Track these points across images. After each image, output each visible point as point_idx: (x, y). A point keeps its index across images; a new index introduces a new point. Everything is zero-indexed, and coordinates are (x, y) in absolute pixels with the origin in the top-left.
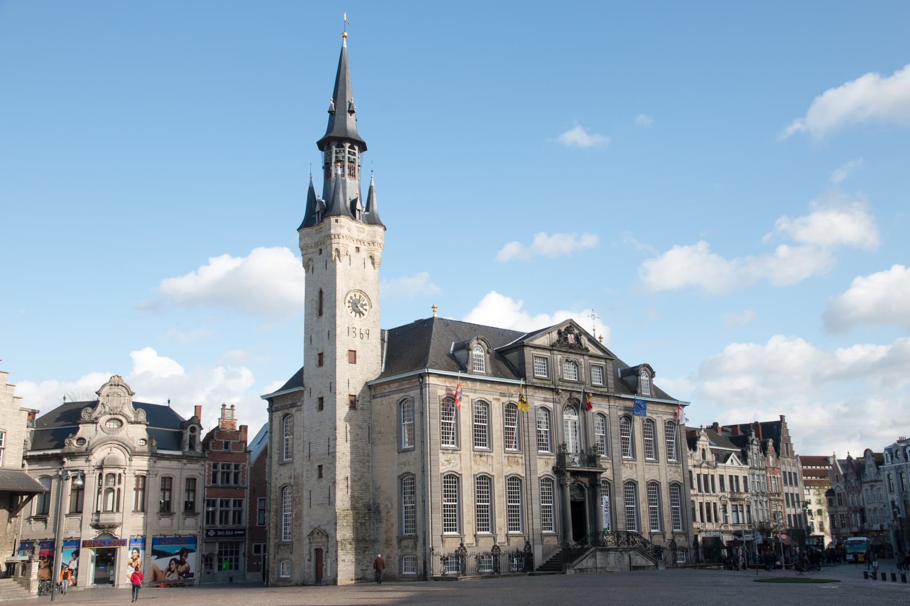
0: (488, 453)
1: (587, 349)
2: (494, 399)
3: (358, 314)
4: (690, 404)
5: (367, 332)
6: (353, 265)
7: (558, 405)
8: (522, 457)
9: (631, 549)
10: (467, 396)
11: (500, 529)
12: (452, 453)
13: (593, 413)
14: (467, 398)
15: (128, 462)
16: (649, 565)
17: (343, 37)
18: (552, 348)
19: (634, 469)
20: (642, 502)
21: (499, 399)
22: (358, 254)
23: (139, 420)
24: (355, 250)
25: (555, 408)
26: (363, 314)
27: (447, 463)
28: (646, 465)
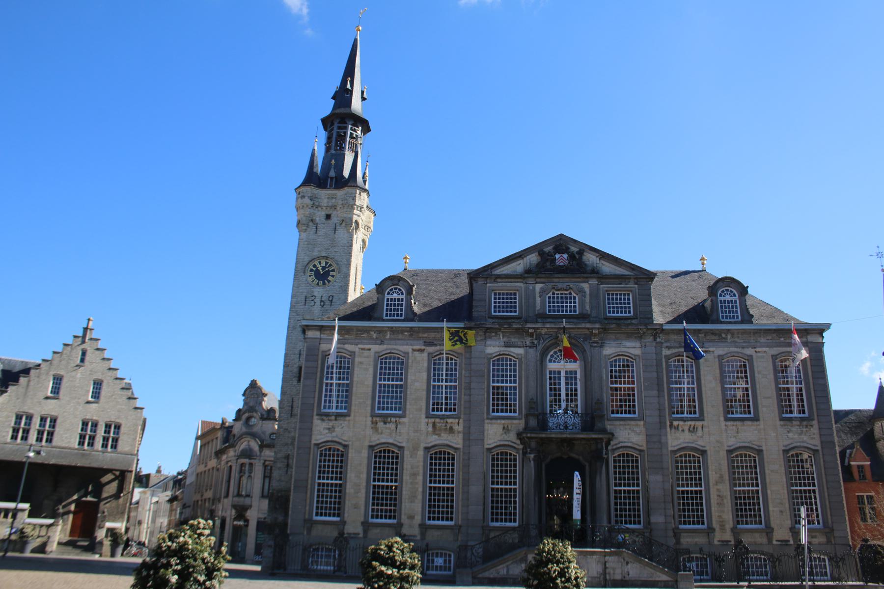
0: (397, 419)
2: (414, 350)
3: (321, 283)
4: (832, 327)
5: (331, 298)
6: (321, 232)
7: (532, 351)
8: (458, 423)
11: (411, 517)
12: (336, 420)
13: (605, 355)
14: (368, 351)
16: (660, 579)
17: (357, 31)
18: (530, 273)
19: (700, 433)
20: (717, 483)
21: (424, 350)
22: (329, 221)
24: (323, 218)
25: (526, 353)
26: (329, 281)
27: (327, 431)
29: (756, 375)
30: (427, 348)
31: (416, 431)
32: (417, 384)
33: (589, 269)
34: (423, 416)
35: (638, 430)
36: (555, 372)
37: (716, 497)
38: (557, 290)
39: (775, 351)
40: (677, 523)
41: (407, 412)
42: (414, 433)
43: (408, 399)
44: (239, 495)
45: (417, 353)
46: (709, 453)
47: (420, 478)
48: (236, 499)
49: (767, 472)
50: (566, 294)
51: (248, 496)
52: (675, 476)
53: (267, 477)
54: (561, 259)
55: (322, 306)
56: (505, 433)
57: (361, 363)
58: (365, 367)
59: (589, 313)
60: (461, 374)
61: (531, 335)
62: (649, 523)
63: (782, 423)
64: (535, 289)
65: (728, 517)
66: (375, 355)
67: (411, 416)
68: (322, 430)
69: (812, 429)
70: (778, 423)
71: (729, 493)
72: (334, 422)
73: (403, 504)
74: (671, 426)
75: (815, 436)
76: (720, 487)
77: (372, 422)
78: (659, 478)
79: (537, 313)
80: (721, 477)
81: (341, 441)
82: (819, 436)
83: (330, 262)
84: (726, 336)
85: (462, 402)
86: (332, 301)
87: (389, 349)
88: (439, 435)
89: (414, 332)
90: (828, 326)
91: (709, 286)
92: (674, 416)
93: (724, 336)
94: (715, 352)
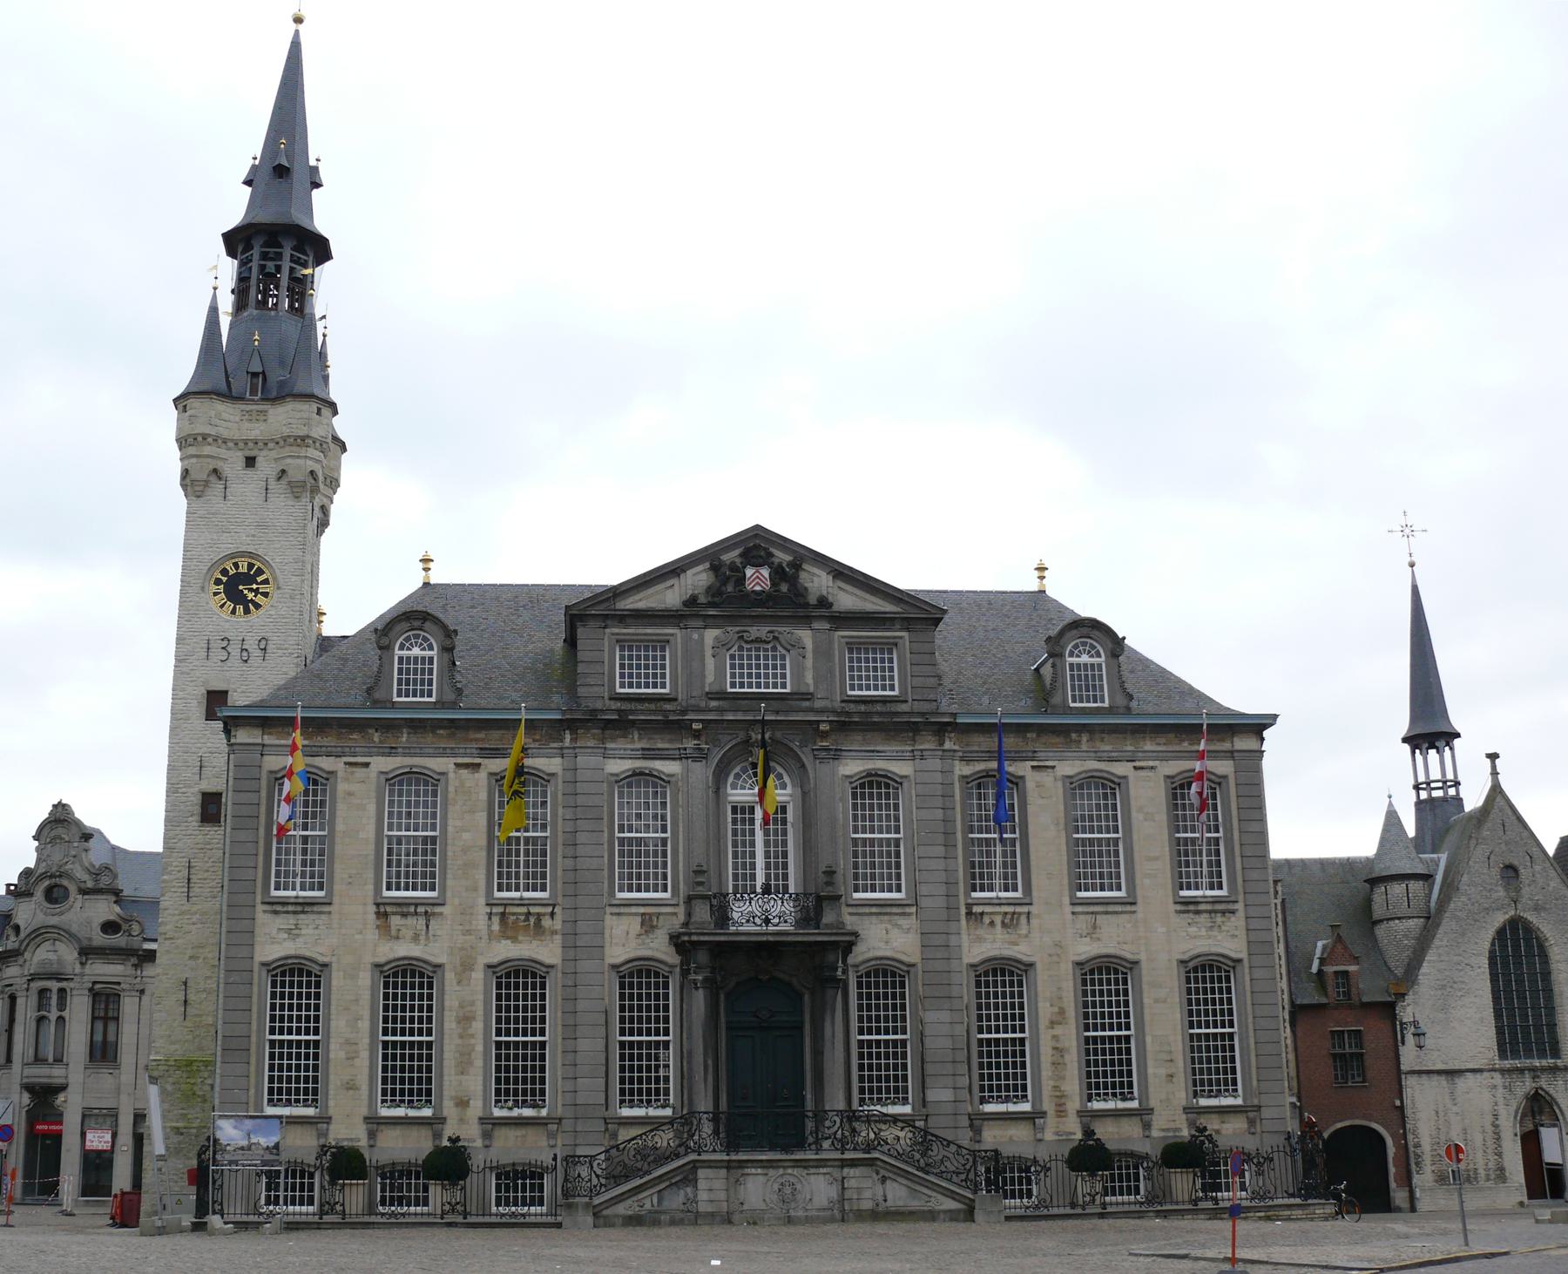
1: (823, 602)
2: (457, 765)
3: (240, 608)
8: (552, 914)
9: (853, 1163)
10: (367, 765)
11: (462, 1103)
14: (364, 770)
15: (78, 966)
20: (1053, 1024)
21: (479, 765)
23: (101, 886)
26: (257, 606)
27: (286, 936)
28: (1073, 913)
29: (1134, 814)
30: (486, 761)
31: (468, 932)
32: (466, 836)
33: (812, 600)
34: (482, 901)
35: (903, 921)
36: (743, 809)
37: (1050, 1051)
38: (747, 642)
39: (1174, 767)
40: (977, 1100)
41: (449, 894)
42: (464, 935)
43: (449, 866)
44: (38, 1060)
45: (464, 772)
46: (1039, 966)
47: (478, 1026)
48: (29, 1071)
49: (1146, 1001)
50: (767, 650)
51: (58, 1060)
52: (974, 1012)
53: (99, 1018)
54: (757, 579)
55: (246, 661)
56: (646, 931)
57: (350, 794)
58: (359, 801)
59: (811, 690)
60: (554, 814)
61: (697, 735)
62: (924, 1103)
63: (1179, 907)
64: (703, 639)
65: (1073, 1085)
66: (378, 777)
67: (457, 901)
68: (275, 931)
69: (1233, 919)
70: (1173, 907)
71: (1074, 1043)
72: (302, 916)
73: (446, 1078)
74: (969, 914)
75: (1236, 933)
76: (1058, 1030)
77: (378, 914)
78: (945, 1016)
79: (707, 690)
80: (1062, 1012)
81: (314, 955)
82: (1244, 932)
83: (258, 564)
84: (1080, 736)
85: (560, 873)
86: (265, 649)
87: (407, 766)
88: (514, 939)
89: (457, 728)
90: (1271, 719)
91: (1050, 638)
92: (974, 895)
93: (1074, 736)
94: (1057, 768)
